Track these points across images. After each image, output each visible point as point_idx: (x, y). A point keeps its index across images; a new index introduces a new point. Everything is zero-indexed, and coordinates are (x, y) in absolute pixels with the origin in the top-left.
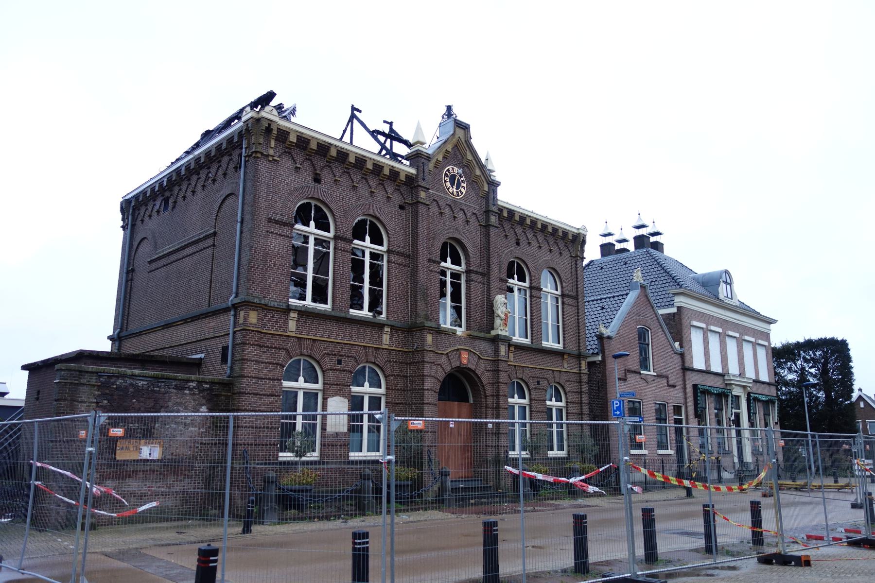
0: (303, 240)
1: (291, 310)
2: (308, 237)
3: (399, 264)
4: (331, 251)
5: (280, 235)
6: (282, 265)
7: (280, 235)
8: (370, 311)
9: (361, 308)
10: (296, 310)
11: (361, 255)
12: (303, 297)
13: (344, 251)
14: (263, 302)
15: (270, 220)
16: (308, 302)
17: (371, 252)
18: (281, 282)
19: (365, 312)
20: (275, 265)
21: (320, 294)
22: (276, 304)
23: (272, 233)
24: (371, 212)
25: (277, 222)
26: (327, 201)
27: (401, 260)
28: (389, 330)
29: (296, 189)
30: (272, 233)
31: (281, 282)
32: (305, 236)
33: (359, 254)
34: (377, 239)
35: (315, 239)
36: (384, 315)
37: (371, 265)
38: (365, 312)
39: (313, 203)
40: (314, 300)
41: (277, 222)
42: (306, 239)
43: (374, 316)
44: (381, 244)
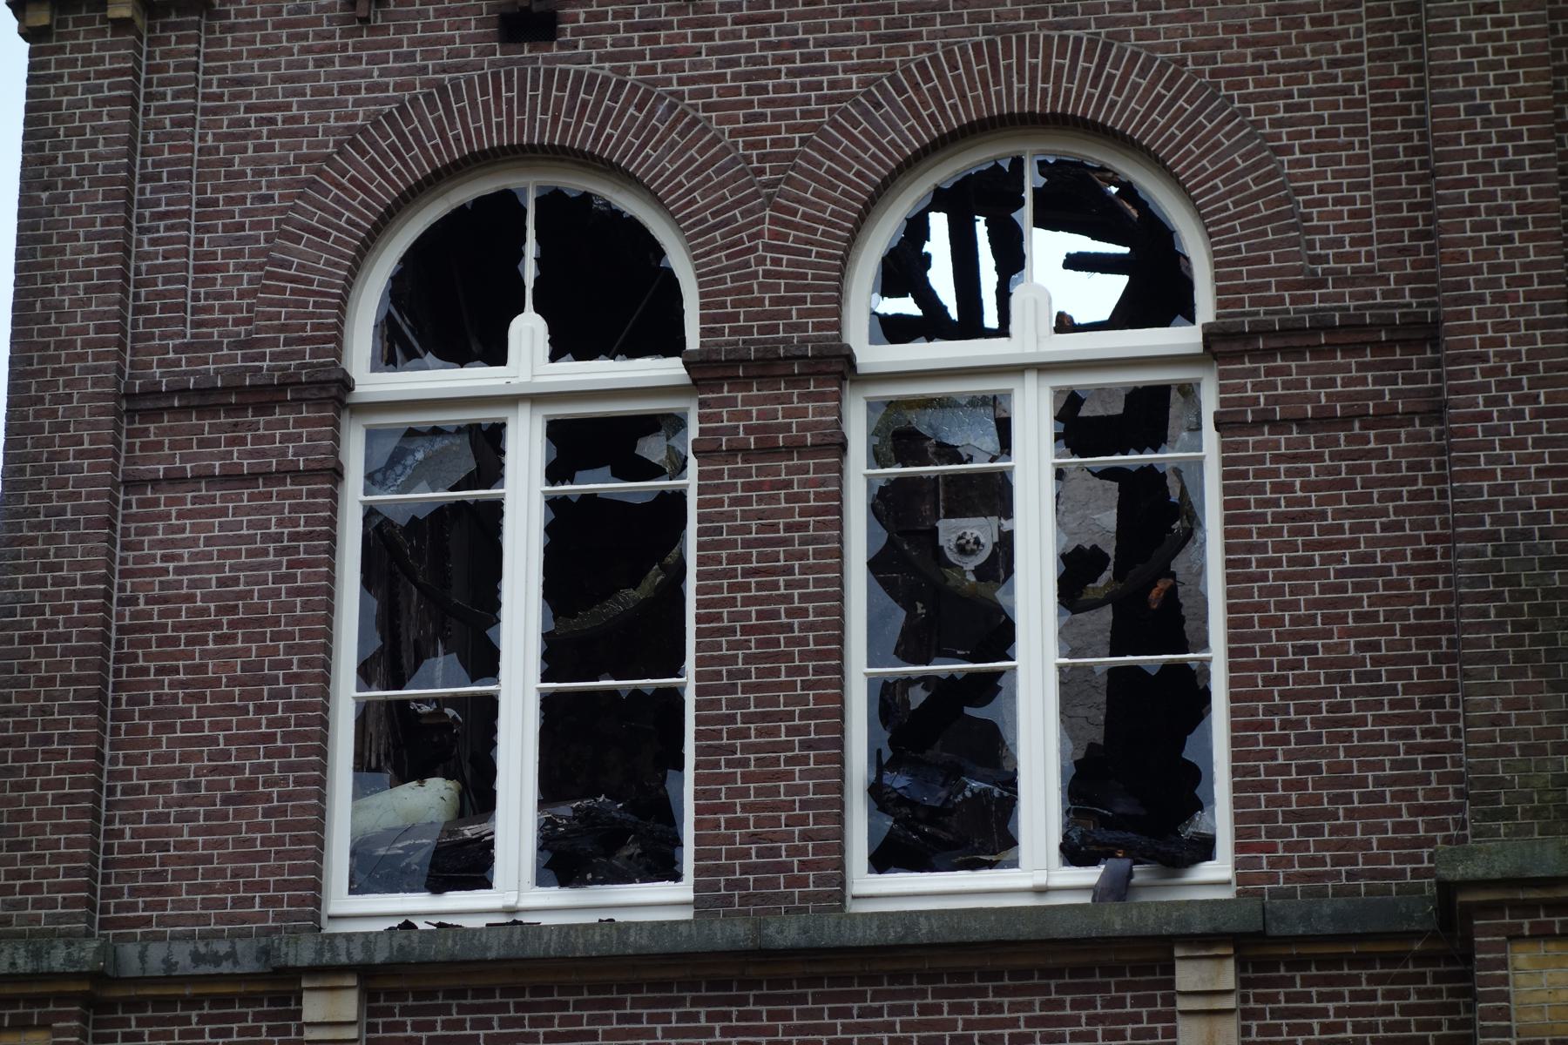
5: (232, 478)
6: (254, 676)
7: (232, 478)
8: (1073, 853)
11: (991, 443)
12: (465, 863)
13: (768, 450)
14: (57, 959)
15: (140, 405)
18: (246, 794)
19: (1039, 867)
20: (198, 685)
21: (609, 803)
22: (182, 956)
23: (175, 479)
24: (1012, 95)
25: (205, 399)
26: (615, 141)
27: (1349, 377)
28: (1226, 977)
29: (353, 139)
30: (175, 479)
31: (246, 794)
32: (473, 429)
33: (977, 438)
36: (1219, 869)
38: (1039, 867)
39: (529, 186)
40: (562, 862)
41: (205, 399)
43: (1115, 890)
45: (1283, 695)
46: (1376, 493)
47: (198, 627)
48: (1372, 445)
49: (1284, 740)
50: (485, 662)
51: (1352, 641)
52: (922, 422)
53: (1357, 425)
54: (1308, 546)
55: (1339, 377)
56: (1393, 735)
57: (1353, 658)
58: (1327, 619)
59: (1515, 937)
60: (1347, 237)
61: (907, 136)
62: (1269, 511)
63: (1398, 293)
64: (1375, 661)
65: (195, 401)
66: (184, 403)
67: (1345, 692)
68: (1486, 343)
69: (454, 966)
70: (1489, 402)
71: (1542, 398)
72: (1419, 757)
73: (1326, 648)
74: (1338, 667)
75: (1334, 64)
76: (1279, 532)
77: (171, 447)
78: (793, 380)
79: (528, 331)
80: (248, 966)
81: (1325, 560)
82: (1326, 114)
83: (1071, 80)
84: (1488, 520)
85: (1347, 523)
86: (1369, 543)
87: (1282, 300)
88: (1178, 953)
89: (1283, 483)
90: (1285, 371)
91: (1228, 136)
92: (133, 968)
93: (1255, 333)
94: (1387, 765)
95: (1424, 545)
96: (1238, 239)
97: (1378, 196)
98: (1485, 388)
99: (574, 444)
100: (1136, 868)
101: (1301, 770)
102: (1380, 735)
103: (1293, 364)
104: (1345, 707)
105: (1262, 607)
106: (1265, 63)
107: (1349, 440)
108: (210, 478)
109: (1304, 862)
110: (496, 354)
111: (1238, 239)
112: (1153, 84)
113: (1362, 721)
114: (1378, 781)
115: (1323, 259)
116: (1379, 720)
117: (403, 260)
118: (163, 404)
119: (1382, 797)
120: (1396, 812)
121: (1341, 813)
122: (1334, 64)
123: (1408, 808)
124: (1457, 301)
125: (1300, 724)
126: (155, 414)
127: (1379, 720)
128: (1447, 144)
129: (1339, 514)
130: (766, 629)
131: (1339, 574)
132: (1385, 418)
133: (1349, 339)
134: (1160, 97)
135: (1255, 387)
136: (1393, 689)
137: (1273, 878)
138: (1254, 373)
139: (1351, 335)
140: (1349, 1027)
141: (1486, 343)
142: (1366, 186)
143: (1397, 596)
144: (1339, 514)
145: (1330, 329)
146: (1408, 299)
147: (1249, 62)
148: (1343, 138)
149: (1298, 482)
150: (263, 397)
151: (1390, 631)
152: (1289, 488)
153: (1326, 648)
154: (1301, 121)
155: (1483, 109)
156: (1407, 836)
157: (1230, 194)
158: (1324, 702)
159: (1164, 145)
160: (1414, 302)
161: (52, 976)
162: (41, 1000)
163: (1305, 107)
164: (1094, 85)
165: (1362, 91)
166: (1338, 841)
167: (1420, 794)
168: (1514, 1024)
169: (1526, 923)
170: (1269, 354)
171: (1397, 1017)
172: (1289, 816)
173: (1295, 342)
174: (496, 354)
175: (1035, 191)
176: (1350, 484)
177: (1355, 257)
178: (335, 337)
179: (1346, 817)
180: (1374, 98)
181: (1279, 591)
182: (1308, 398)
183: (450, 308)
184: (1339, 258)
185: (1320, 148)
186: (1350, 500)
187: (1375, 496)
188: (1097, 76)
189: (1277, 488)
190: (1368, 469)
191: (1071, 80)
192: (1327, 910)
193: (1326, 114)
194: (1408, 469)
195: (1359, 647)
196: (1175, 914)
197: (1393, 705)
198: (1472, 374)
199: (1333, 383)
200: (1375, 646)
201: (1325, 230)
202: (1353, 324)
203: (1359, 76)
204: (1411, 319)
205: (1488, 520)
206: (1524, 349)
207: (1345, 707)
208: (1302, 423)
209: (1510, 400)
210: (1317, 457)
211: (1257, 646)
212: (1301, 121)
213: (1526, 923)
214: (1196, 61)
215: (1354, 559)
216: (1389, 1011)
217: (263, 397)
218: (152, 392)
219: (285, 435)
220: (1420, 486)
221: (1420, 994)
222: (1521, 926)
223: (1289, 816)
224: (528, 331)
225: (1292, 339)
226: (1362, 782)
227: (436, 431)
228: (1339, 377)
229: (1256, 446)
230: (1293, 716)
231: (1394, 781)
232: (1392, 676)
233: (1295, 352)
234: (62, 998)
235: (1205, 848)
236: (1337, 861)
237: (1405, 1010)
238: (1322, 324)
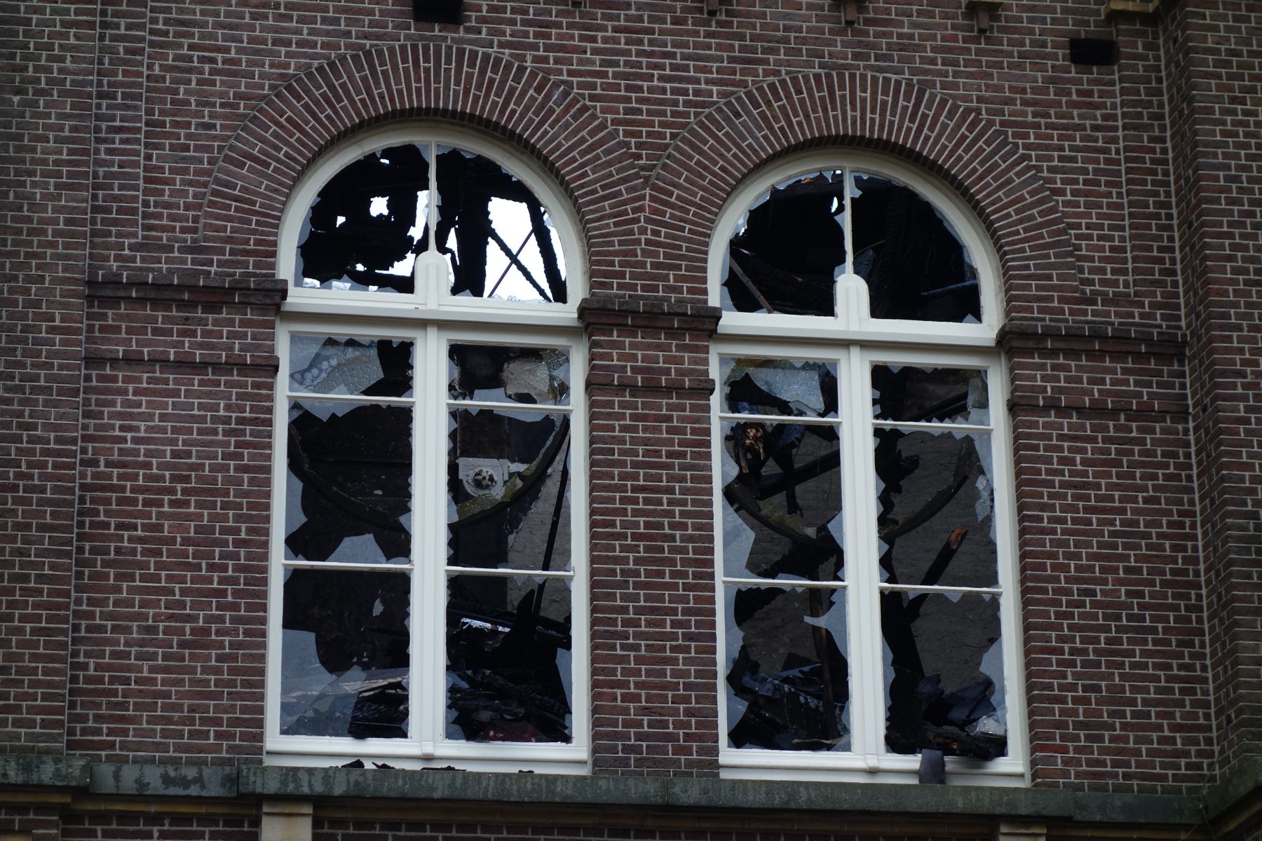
0: (376, 373)
1: (258, 800)
2: (406, 348)
3: (1097, 410)
4: (577, 406)
5: (184, 365)
6: (205, 538)
7: (184, 365)
8: (896, 742)
9: (826, 729)
10: (298, 793)
11: (818, 401)
12: (386, 714)
13: (652, 388)
14: (46, 773)
15: (102, 292)
16: (427, 737)
17: (880, 375)
18: (200, 641)
19: (865, 752)
20: (155, 542)
21: (507, 675)
22: (153, 778)
23: (132, 360)
24: (845, 120)
25: (160, 294)
26: (515, 116)
27: (1110, 379)
29: (288, 86)
30: (132, 360)
31: (200, 641)
32: (384, 346)
34: (920, 276)
35: (457, 353)
36: (1013, 763)
37: (892, 459)
39: (432, 145)
40: (466, 720)
41: (160, 294)
42: (396, 364)
43: (933, 774)
44: (965, 305)
45: (1070, 628)
46: (1138, 472)
47: (154, 492)
48: (1134, 434)
49: (1072, 664)
50: (398, 544)
51: (1123, 589)
52: (761, 378)
53: (1122, 417)
55: (1108, 378)
57: (1123, 602)
58: (1103, 570)
60: (1109, 267)
61: (761, 141)
62: (1057, 479)
63: (1151, 316)
65: (152, 295)
66: (141, 295)
67: (1118, 630)
69: (405, 803)
72: (1177, 686)
73: (1103, 592)
74: (1113, 609)
75: (1095, 128)
76: (1064, 497)
77: (130, 333)
78: (672, 333)
79: (851, 288)
80: (214, 790)
82: (1090, 167)
83: (893, 114)
84: (1250, 503)
85: (1117, 494)
87: (1062, 312)
88: (1004, 829)
89: (1066, 458)
90: (1066, 368)
91: (1018, 175)
92: (108, 786)
93: (1045, 335)
94: (1152, 690)
95: (1176, 518)
96: (1028, 258)
97: (1132, 237)
99: (895, 390)
100: (946, 758)
101: (1086, 688)
103: (1073, 363)
104: (1118, 641)
105: (1053, 556)
106: (1043, 121)
107: (1117, 428)
108: (164, 363)
109: (1090, 763)
110: (826, 308)
111: (1028, 258)
112: (958, 127)
115: (1090, 282)
116: (1145, 653)
117: (321, 194)
118: (122, 294)
119: (1148, 715)
120: (1159, 728)
122: (1095, 128)
123: (1169, 725)
124: (1222, 327)
125: (1084, 652)
126: (113, 302)
127: (1145, 653)
128: (1211, 203)
130: (652, 536)
131: (1113, 534)
132: (1144, 414)
133: (1118, 348)
134: (964, 137)
135: (1043, 378)
137: (1066, 774)
138: (1042, 367)
139: (1115, 344)
141: (1245, 362)
142: (1122, 228)
143: (1157, 556)
144: (1110, 487)
145: (1103, 338)
146: (1159, 322)
147: (1030, 118)
148: (1103, 188)
149: (1078, 457)
150: (214, 297)
152: (1071, 462)
153: (1103, 592)
154: (1072, 171)
155: (1236, 179)
156: (1169, 748)
157: (1021, 221)
158: (1103, 636)
159: (968, 176)
160: (1164, 324)
161: (41, 788)
162: (23, 809)
163: (1074, 160)
164: (912, 120)
165: (1118, 152)
167: (1178, 715)
170: (1053, 353)
172: (1078, 725)
173: (1076, 346)
174: (826, 308)
175: (852, 199)
177: (1115, 283)
178: (270, 252)
180: (1127, 160)
181: (1065, 544)
183: (784, 263)
184: (1103, 282)
185: (1086, 194)
186: (1119, 476)
187: (1138, 475)
188: (914, 115)
189: (1062, 461)
190: (1132, 453)
191: (893, 114)
192: (1118, 803)
193: (1090, 167)
195: (1128, 593)
196: (1005, 799)
197: (1155, 642)
198: (1234, 386)
199: (1103, 382)
200: (1140, 594)
201: (1092, 259)
202: (1121, 337)
203: (1115, 140)
204: (1166, 337)
205: (1250, 503)
207: (1118, 641)
208: (1081, 411)
210: (1093, 440)
211: (1050, 586)
212: (1072, 171)
214: (988, 112)
215: (1123, 523)
217: (214, 297)
218: (113, 281)
219: (226, 332)
220: (1172, 470)
223: (1078, 725)
224: (851, 288)
225: (1076, 343)
226: (1133, 702)
227: (351, 343)
228: (1108, 378)
229: (1046, 425)
230: (1078, 645)
231: (1157, 703)
233: (1073, 354)
234: (42, 808)
235: (998, 746)
236: (1115, 764)
238: (1098, 334)
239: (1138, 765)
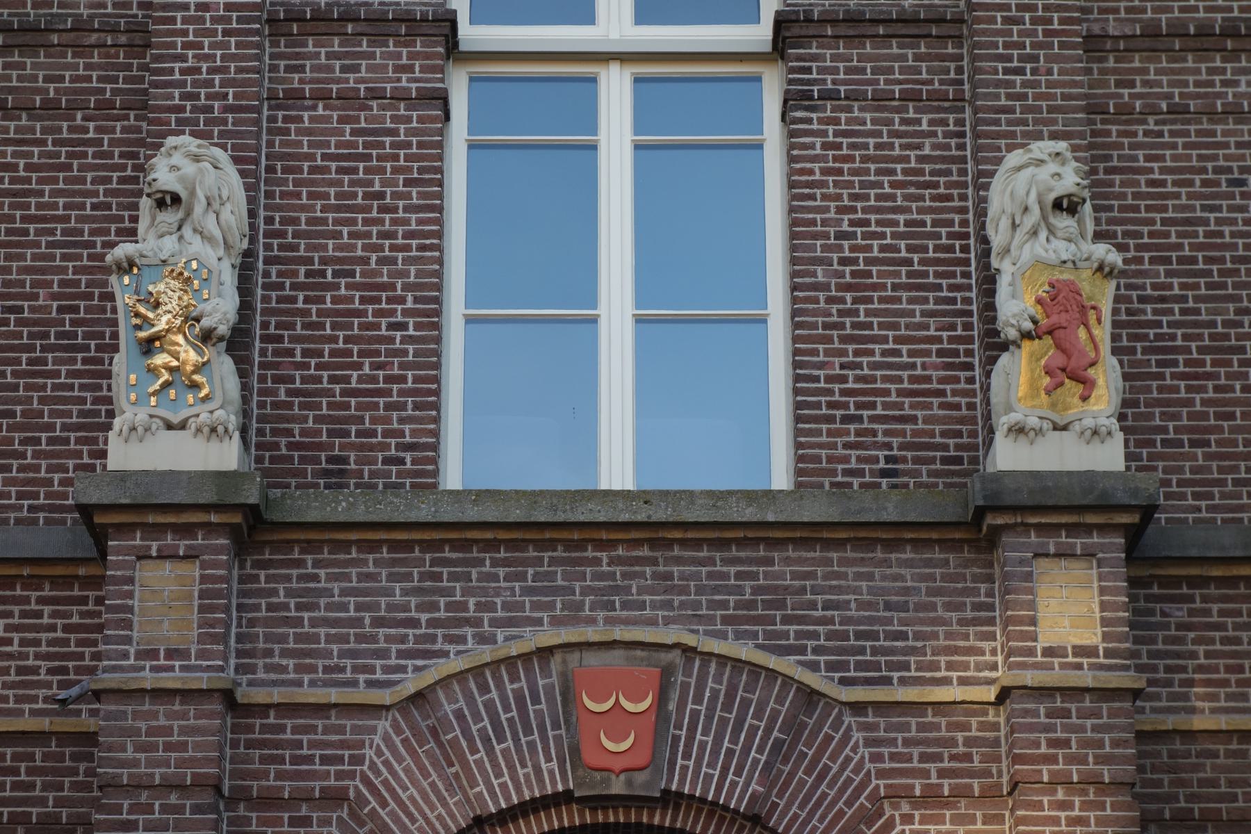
54: (24, 219)
56: (83, 387)
59: (143, 556)
64: (74, 323)
68: (186, 46)
70: (184, 97)
71: (230, 97)
73: (32, 309)
81: (38, 232)
86: (80, 219)
90: (22, 66)
98: (182, 84)
102: (71, 388)
103: (29, 61)
107: (71, 129)
113: (57, 374)
114: (65, 428)
116: (72, 374)
120: (79, 454)
121: (29, 454)
127: (71, 374)
129: (54, 193)
131: (50, 245)
136: (86, 348)
140: (16, 642)
144: (56, 193)
146: (135, 11)
149: (22, 163)
151: (90, 296)
153: (32, 309)
158: (25, 356)
160: (140, 13)
166: (25, 479)
168: (135, 634)
169: (155, 546)
171: (59, 634)
176: (68, 167)
179: (33, 458)
182: (38, 91)
187: (89, 180)
194: (120, 157)
197: (85, 361)
199: (61, 79)
200: (75, 310)
206: (219, 53)
209: (203, 96)
210: (43, 143)
213: (155, 546)
215: (65, 232)
216: (52, 628)
220: (129, 172)
221: (83, 615)
222: (149, 547)
226: (50, 427)
228: (67, 74)
232: (87, 336)
236: (20, 496)
237: (66, 628)
239: (48, 496)
